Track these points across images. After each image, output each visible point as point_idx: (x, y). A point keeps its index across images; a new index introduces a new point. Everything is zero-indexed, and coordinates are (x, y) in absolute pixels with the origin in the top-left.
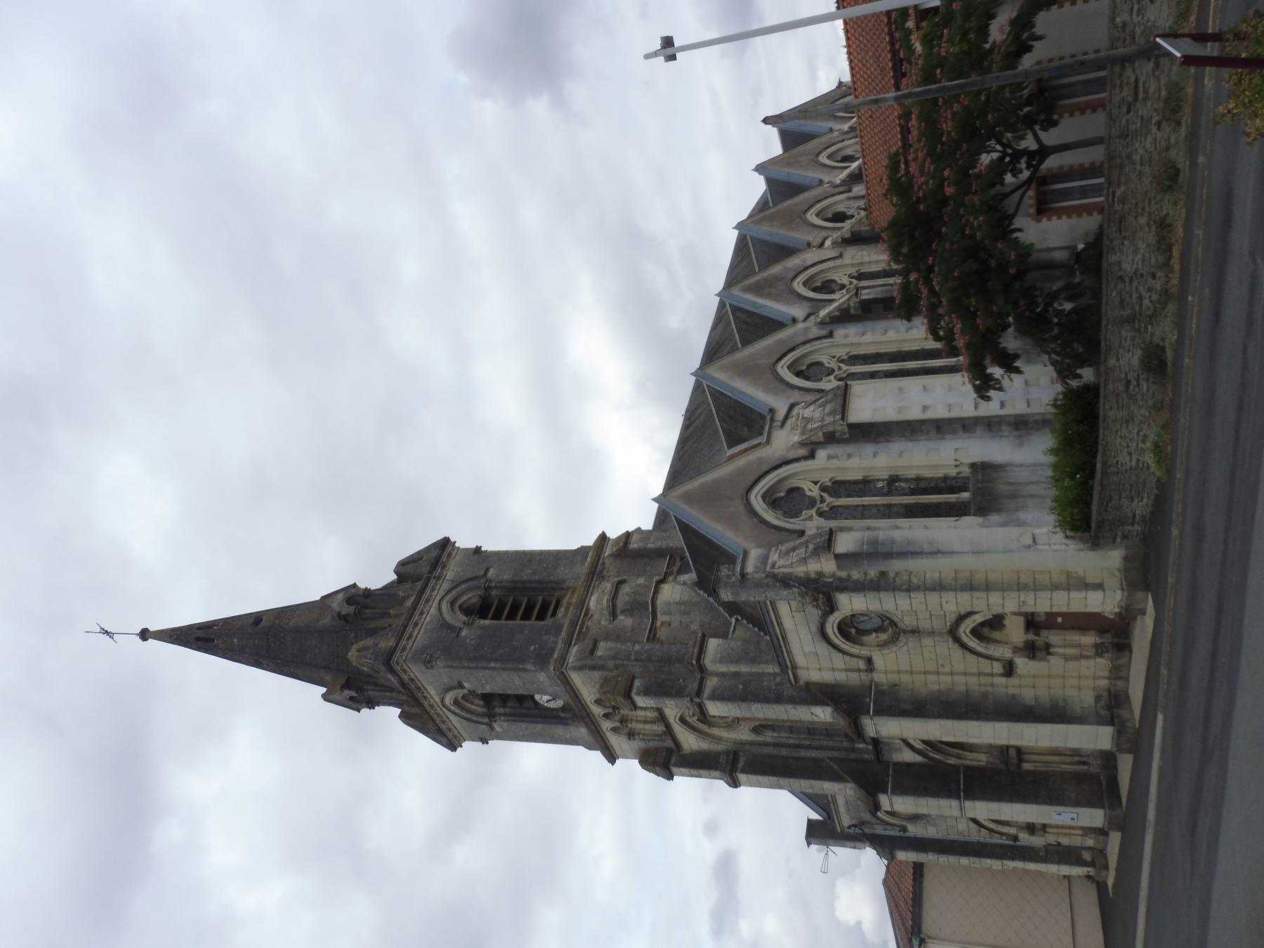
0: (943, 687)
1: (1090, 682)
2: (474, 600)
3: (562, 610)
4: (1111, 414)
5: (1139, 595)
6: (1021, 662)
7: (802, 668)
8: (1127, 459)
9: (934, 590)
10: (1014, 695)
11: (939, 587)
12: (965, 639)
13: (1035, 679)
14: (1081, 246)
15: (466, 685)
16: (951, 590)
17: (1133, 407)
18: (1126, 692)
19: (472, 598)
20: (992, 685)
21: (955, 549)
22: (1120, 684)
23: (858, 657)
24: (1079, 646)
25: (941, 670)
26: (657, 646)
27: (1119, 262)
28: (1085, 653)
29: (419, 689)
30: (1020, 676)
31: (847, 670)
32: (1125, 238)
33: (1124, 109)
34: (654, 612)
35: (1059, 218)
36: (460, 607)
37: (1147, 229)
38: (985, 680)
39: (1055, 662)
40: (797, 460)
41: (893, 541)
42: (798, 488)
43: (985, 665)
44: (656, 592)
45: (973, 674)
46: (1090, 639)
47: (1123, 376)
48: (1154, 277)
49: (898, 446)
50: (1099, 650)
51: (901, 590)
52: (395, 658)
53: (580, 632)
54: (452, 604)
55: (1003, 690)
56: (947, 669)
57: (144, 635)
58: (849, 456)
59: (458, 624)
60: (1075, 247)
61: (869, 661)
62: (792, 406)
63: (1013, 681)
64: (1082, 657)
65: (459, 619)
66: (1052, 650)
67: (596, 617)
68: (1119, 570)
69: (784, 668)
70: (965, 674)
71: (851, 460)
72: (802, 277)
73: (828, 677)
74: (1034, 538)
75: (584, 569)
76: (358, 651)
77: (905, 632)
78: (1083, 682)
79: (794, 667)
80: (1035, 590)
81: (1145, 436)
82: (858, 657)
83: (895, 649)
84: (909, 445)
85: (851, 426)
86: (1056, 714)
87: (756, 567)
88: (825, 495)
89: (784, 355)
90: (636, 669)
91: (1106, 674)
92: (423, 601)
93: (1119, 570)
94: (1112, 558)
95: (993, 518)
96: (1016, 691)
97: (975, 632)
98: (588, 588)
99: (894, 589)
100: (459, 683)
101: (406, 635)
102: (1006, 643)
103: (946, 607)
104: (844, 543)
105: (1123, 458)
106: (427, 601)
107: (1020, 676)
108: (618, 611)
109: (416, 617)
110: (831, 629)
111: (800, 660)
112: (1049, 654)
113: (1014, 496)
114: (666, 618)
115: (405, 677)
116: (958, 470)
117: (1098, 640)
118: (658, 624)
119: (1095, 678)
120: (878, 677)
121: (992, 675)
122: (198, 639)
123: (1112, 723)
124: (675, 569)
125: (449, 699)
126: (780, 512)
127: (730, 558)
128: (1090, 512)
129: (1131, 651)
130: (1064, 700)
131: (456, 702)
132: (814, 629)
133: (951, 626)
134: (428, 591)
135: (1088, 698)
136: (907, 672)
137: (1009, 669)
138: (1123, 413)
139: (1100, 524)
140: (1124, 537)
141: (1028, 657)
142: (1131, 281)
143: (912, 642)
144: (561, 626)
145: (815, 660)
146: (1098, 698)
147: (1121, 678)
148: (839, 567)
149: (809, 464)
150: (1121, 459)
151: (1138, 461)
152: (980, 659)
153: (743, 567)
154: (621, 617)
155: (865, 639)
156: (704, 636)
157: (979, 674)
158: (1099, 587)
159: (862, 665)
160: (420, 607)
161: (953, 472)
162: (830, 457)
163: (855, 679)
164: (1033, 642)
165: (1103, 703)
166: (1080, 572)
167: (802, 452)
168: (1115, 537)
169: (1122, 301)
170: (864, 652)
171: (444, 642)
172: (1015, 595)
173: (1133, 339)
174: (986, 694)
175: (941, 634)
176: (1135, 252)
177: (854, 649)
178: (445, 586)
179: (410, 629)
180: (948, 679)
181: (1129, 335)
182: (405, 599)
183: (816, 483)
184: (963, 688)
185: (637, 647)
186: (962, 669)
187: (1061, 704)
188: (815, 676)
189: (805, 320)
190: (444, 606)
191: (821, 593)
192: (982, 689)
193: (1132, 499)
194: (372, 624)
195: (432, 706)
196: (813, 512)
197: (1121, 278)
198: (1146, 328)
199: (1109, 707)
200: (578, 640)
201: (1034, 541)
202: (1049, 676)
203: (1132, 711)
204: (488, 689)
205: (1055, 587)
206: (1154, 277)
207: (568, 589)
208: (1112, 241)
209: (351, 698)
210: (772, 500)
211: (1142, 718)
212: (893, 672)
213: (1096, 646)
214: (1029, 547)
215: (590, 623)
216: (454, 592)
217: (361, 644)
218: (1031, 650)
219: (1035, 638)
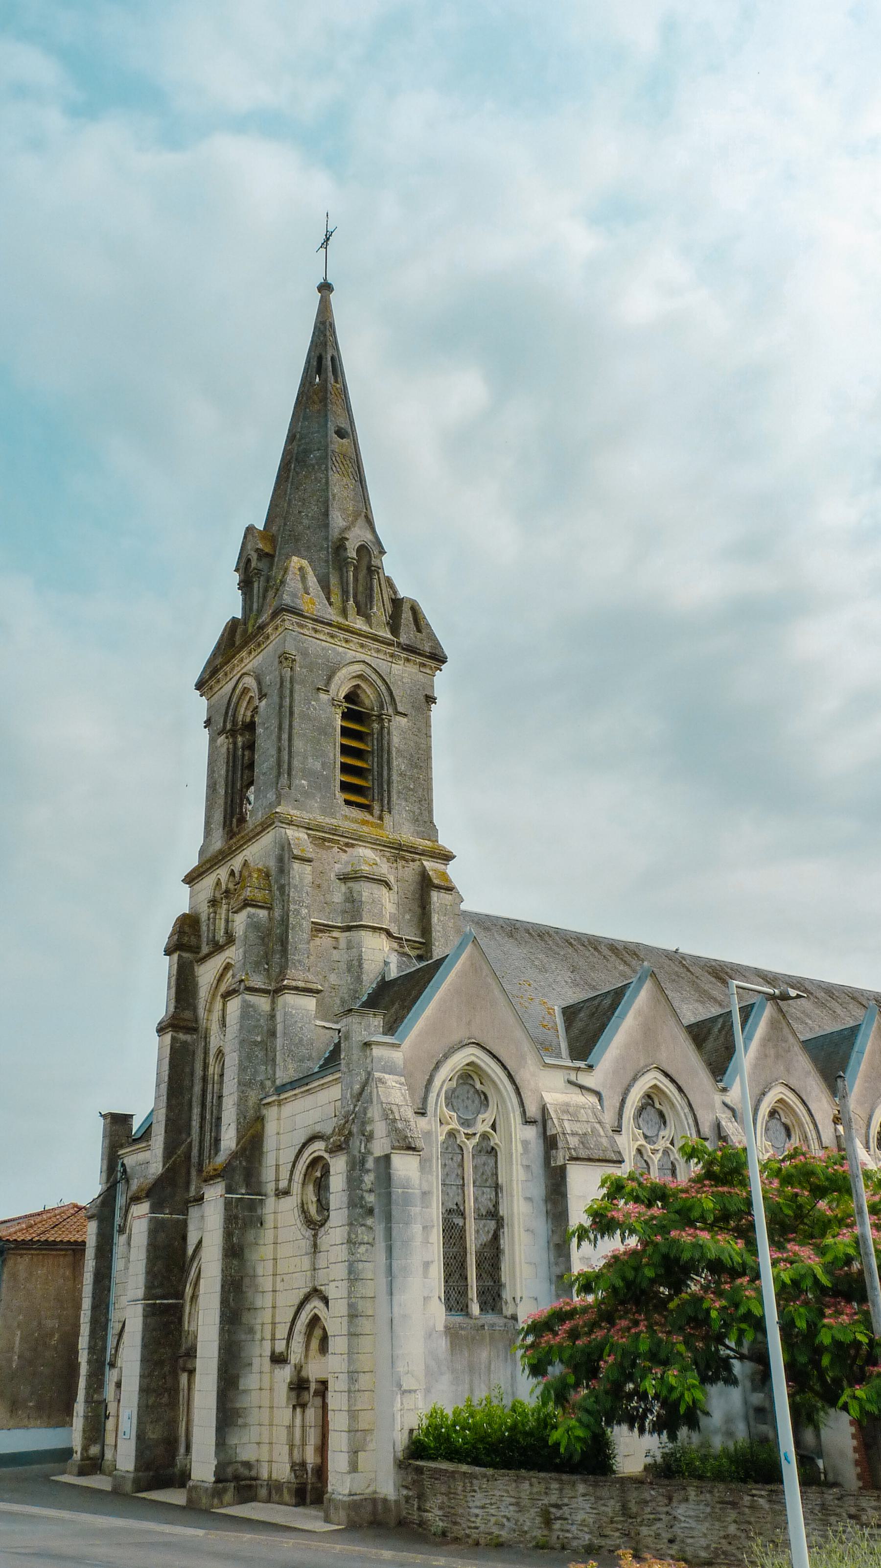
0: (260, 1280)
1: (265, 1457)
2: (367, 702)
3: (355, 813)
4: (526, 1486)
5: (342, 1514)
6: (285, 1374)
7: (279, 1113)
8: (478, 1504)
9: (350, 1272)
10: (250, 1364)
11: (353, 1277)
12: (308, 1307)
13: (266, 1389)
14: (820, 1463)
15: (264, 702)
16: (350, 1293)
17: (533, 1511)
18: (254, 1499)
19: (369, 697)
20: (263, 1339)
21: (396, 1298)
22: (263, 1492)
23: (290, 1180)
24: (304, 1444)
25: (279, 1278)
26: (305, 936)
27: (687, 1500)
28: (296, 1452)
29: (259, 645)
30: (272, 1372)
31: (277, 1166)
32: (713, 1507)
33: (853, 1511)
34: (349, 929)
35: (854, 1436)
36: (358, 686)
37: (722, 1534)
38: (268, 1328)
39: (284, 1415)
40: (522, 1104)
41: (407, 1224)
42: (487, 1105)
43: (282, 1332)
44: (374, 929)
45: (273, 1316)
46: (311, 1458)
47: (566, 1501)
48: (671, 1541)
49: (541, 1226)
50: (299, 1467)
51: (349, 1234)
52: (287, 616)
53: (324, 839)
54: (360, 677)
55: (257, 1351)
56: (279, 1286)
57: (325, 288)
58: (527, 1167)
59: (333, 687)
60: (820, 1456)
61: (287, 1193)
62: (598, 1094)
63: (267, 1361)
64: (292, 1446)
65: (341, 687)
66: (298, 1410)
67: (344, 857)
68: (375, 1492)
69: (280, 1089)
70: (274, 1307)
71: (521, 1170)
72: (791, 1099)
73: (270, 1143)
74: (410, 1391)
75: (407, 835)
76: (301, 569)
77: (315, 1236)
78: (265, 1448)
79: (280, 1103)
80: (349, 1391)
81: (503, 1525)
82: (290, 1180)
83: (299, 1224)
84: (543, 1242)
85: (562, 1170)
86: (228, 1416)
87: (380, 1059)
88: (477, 1139)
89: (673, 1081)
90: (277, 913)
91: (274, 1477)
92: (363, 640)
93: (375, 1492)
94: (387, 1485)
95: (443, 1344)
96: (256, 1367)
97: (315, 1320)
98: (377, 844)
99: (351, 1224)
100: (265, 695)
101: (319, 627)
102: (306, 1356)
103: (333, 1285)
104: (405, 1166)
105: (480, 1499)
106: (362, 646)
107: (272, 1372)
108: (350, 884)
109: (342, 635)
110: (318, 1148)
111: (287, 1110)
112: (294, 1407)
113: (472, 1369)
114: (343, 944)
115: (269, 630)
116: (510, 1300)
117: (309, 1467)
118: (335, 934)
119: (270, 1461)
120: (271, 1202)
121: (273, 1339)
122: (320, 359)
123: (218, 1481)
124: (407, 949)
125: (249, 681)
126: (454, 1083)
127: (391, 1028)
128: (433, 1459)
129: (296, 1505)
130: (245, 1425)
131: (246, 690)
132: (318, 1128)
133: (320, 1292)
134: (376, 645)
135: (246, 1454)
136: (276, 1237)
137: (278, 1359)
138: (525, 1502)
139: (419, 1470)
140: (407, 1499)
141: (291, 1383)
142: (667, 1513)
143: (306, 1245)
144: (333, 815)
145: (293, 1123)
146: (247, 1465)
147: (270, 1494)
148: (377, 1160)
149: (515, 1118)
150: (479, 1495)
151: (477, 1516)
152: (289, 1324)
153: (378, 1044)
154: (343, 888)
155: (310, 1188)
156: (318, 992)
157: (274, 1324)
158: (354, 1468)
159: (283, 1184)
160: (355, 639)
161: (506, 1295)
162: (525, 1143)
163: (268, 1174)
164: (308, 1389)
165: (245, 1472)
166: (371, 1446)
167: (533, 1110)
168: (406, 1487)
169: (646, 1502)
170: (296, 1188)
171: (316, 673)
172: (344, 1367)
173: (605, 1514)
174: (251, 1331)
175: (313, 1277)
176: (697, 1519)
177: (298, 1176)
178: (382, 666)
179: (327, 629)
180: (268, 1287)
181: (608, 1510)
182: (368, 618)
183: (493, 1127)
184: (259, 1303)
185: (304, 911)
186: (280, 1303)
187: (240, 1421)
188: (271, 1128)
189: (725, 1105)
190: (357, 668)
191: (348, 1134)
192: (258, 1327)
193: (440, 1508)
194: (334, 581)
195: (242, 660)
196: (455, 1125)
197: (670, 1499)
198: (618, 1530)
199: (237, 1478)
200: (315, 838)
201: (405, 1391)
202: (272, 1407)
203: (229, 1505)
204: (260, 730)
205: (353, 1415)
206: (671, 1541)
207: (381, 818)
208: (711, 1492)
209: (249, 561)
210: (469, 1075)
211: (57, 1482)
212: (276, 1220)
213: (303, 1464)
214: (400, 1386)
215: (336, 850)
216: (374, 677)
217: (309, 570)
218: (299, 1386)
219: (312, 1390)
